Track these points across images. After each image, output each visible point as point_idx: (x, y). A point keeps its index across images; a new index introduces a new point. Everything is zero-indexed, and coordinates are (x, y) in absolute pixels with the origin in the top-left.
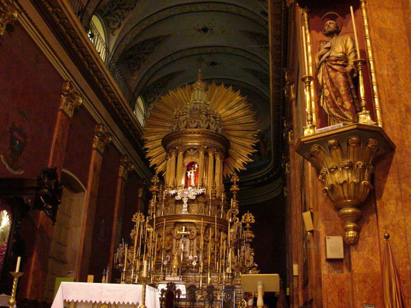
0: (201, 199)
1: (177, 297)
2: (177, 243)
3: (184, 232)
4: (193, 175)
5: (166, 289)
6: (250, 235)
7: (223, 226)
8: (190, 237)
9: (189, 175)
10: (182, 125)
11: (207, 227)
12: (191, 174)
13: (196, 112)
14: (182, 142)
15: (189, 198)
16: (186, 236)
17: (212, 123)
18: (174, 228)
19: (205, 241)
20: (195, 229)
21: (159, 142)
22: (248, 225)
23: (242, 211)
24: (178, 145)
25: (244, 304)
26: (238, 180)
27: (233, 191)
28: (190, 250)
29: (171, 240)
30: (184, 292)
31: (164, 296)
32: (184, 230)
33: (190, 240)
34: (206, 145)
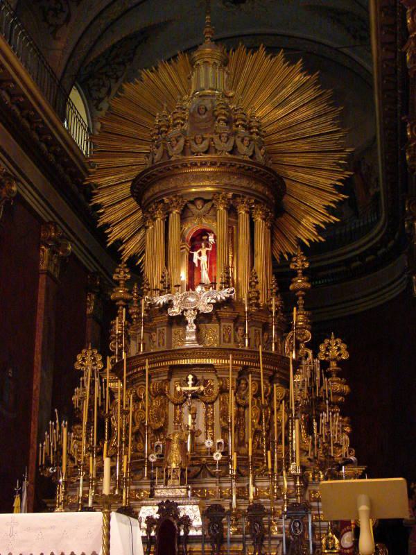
0: (226, 312)
1: (182, 533)
2: (178, 411)
3: (190, 388)
4: (204, 259)
5: (157, 516)
6: (338, 387)
7: (279, 370)
8: (209, 399)
9: (195, 261)
10: (175, 149)
11: (242, 373)
12: (201, 257)
13: (204, 117)
14: (176, 187)
15: (198, 311)
16: (195, 396)
17: (242, 141)
18: (169, 380)
19: (238, 405)
20: (216, 380)
21: (126, 190)
22: (334, 364)
24: (166, 195)
25: (334, 544)
26: (307, 265)
27: (297, 290)
28: (207, 426)
29: (164, 406)
30: (197, 522)
31: (153, 534)
32: (190, 382)
33: (206, 404)
34: (229, 190)
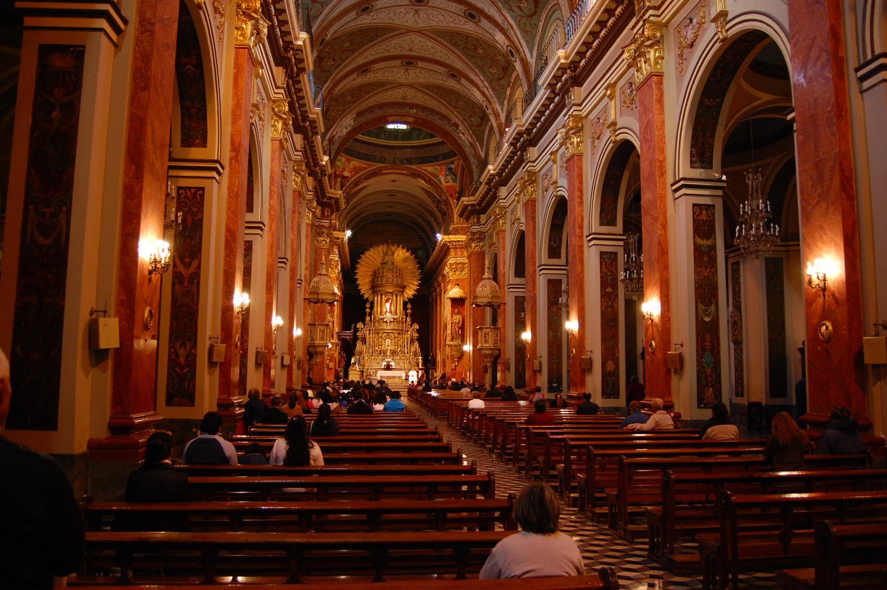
12: (388, 305)
23: (412, 323)
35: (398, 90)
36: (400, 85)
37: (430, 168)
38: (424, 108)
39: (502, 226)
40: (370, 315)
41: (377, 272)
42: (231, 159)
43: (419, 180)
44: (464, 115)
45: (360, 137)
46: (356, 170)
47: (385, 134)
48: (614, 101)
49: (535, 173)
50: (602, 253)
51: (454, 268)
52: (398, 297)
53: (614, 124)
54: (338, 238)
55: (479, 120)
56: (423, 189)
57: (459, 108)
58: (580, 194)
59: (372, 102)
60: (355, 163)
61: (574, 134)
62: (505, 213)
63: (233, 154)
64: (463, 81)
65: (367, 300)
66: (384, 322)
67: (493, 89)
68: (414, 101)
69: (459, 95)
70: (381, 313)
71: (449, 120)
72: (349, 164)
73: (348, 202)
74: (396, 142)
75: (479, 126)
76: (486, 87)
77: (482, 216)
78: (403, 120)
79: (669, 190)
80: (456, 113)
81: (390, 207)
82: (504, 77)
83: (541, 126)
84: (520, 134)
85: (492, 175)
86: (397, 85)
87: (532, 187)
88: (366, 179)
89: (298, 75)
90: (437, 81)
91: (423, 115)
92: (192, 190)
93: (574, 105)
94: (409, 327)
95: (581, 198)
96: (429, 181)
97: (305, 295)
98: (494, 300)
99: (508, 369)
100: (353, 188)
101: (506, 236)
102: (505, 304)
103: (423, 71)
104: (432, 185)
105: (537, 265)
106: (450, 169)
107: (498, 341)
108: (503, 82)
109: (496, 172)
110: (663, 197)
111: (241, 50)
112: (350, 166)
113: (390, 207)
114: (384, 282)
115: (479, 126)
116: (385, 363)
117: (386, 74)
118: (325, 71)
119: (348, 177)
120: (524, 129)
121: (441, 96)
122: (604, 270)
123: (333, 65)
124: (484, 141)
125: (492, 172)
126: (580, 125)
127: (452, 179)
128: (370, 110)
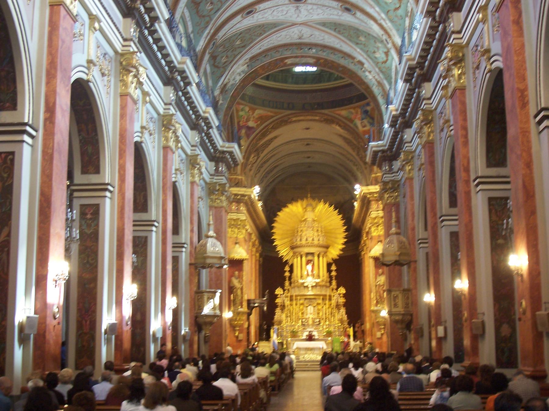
11: (323, 299)
12: (309, 267)
35: (292, 30)
36: (294, 24)
37: (344, 112)
38: (324, 47)
39: (409, 173)
40: (290, 278)
41: (296, 231)
42: (46, 120)
43: (334, 126)
44: (368, 51)
45: (260, 81)
46: (262, 119)
47: (292, 78)
48: (487, 25)
49: (431, 112)
50: (490, 199)
51: (376, 223)
52: (321, 258)
53: (488, 51)
54: (243, 196)
55: (383, 56)
56: (340, 136)
57: (361, 44)
58: (464, 133)
59: (266, 45)
60: (259, 112)
61: (455, 64)
62: (412, 158)
63: (48, 115)
64: (359, 14)
65: (286, 262)
66: (305, 287)
67: (391, 21)
68: (313, 40)
69: (358, 30)
70: (301, 277)
71: (353, 58)
72: (253, 113)
73: (258, 154)
74: (305, 86)
75: (385, 62)
76: (384, 20)
77: (394, 162)
78: (303, 62)
79: (533, 122)
80: (358, 50)
81: (309, 157)
82: (400, 7)
83: (432, 58)
84: (411, 69)
85: (394, 117)
86: (290, 24)
87: (429, 128)
88: (274, 128)
89: (152, 25)
90: (332, 17)
91: (324, 55)
92: (3, 156)
93: (453, 32)
94: (335, 291)
95: (466, 136)
96: (345, 127)
97: (191, 260)
98: (402, 257)
99: (422, 336)
100: (260, 139)
101: (414, 184)
102: (416, 262)
103: (315, 7)
104: (347, 130)
105: (438, 215)
106: (366, 112)
107: (410, 305)
108: (400, 12)
109: (399, 112)
110: (526, 132)
111: (55, 7)
112: (255, 114)
113: (309, 157)
114: (304, 242)
115: (385, 62)
116: (307, 333)
117: (275, 13)
118: (204, 16)
119: (252, 128)
120: (415, 62)
121: (339, 32)
122: (494, 218)
123: (212, 9)
124: (391, 78)
125: (394, 113)
126: (461, 55)
127: (369, 122)
128: (265, 53)
